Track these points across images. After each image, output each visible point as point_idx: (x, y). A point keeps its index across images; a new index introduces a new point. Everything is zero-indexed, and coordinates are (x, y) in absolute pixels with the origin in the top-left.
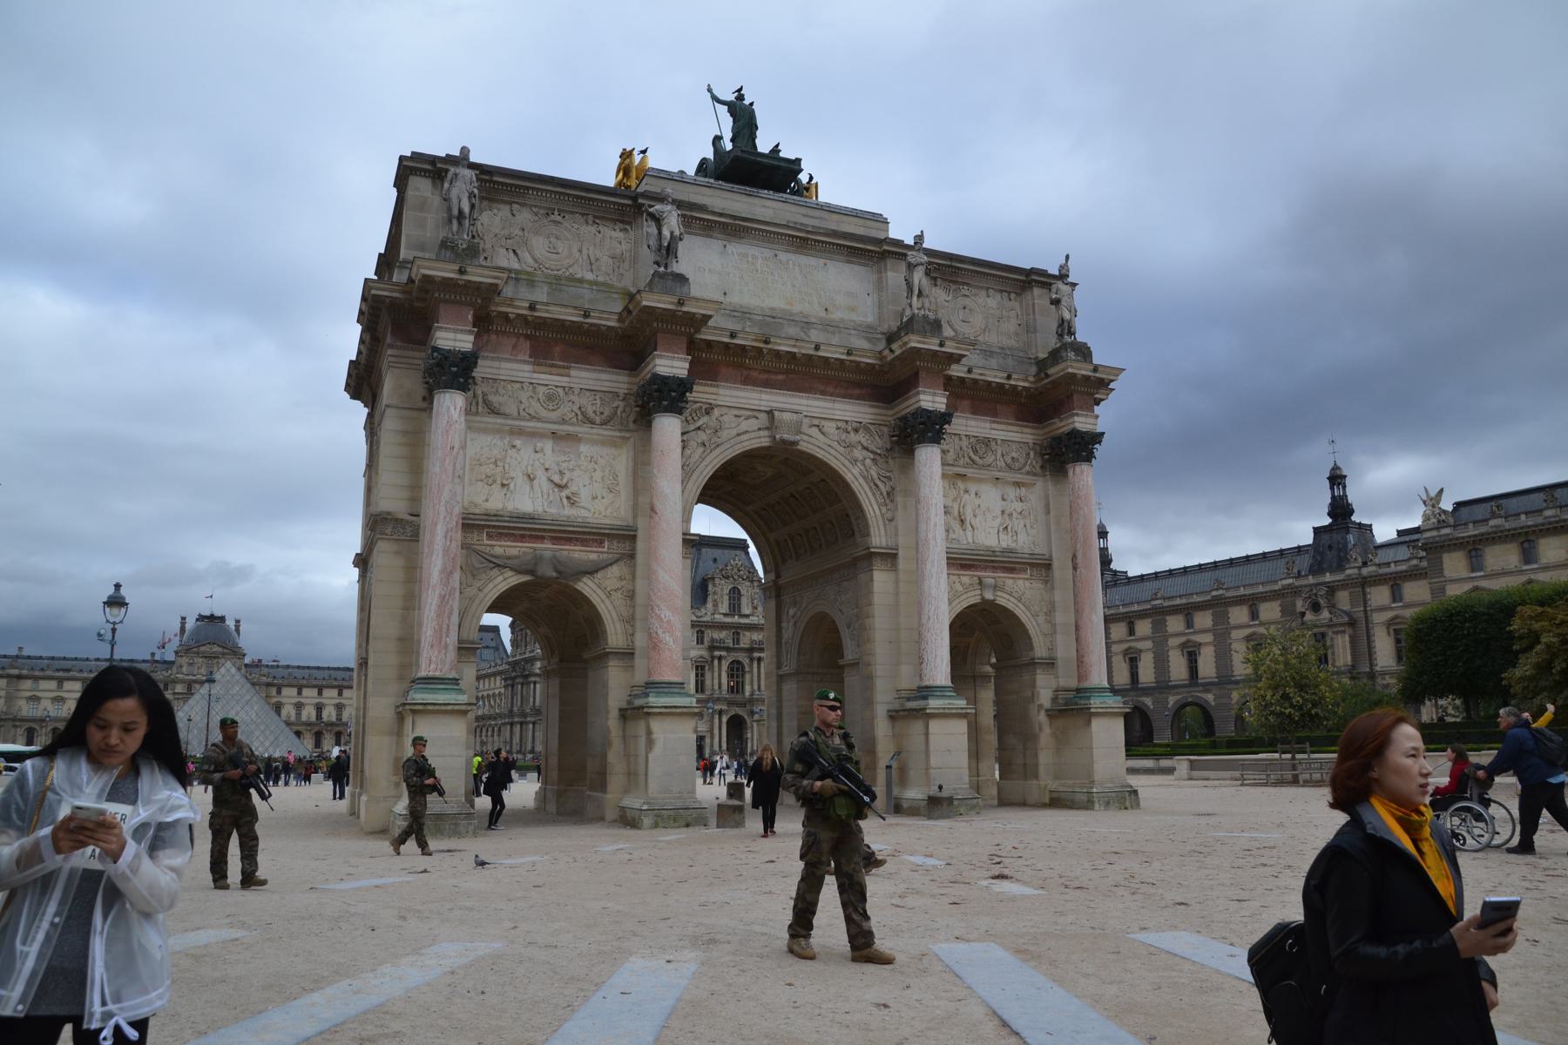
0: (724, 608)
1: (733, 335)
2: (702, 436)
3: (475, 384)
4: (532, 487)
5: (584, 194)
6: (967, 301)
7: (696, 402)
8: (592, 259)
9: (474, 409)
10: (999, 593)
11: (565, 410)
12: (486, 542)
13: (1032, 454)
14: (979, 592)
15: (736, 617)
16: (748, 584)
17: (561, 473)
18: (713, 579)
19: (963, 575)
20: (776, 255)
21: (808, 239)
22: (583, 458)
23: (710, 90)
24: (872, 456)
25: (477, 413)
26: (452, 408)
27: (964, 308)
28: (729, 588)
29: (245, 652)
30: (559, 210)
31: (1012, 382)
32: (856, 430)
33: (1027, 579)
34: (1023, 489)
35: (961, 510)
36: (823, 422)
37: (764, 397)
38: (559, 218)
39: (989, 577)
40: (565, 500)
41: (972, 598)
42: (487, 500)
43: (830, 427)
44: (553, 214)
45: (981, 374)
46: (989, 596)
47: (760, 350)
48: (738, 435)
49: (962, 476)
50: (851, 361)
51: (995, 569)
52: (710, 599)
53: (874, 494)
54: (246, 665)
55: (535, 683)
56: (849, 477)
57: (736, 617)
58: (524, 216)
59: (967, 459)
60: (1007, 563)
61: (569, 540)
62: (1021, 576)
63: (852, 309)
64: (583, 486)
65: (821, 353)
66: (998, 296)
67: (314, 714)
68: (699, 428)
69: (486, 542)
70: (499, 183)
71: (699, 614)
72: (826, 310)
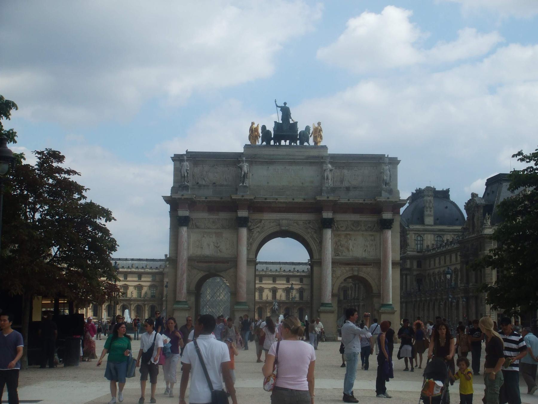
1: (266, 199)
2: (259, 230)
3: (193, 220)
4: (209, 247)
5: (222, 159)
7: (257, 219)
8: (227, 179)
9: (192, 227)
10: (360, 273)
12: (196, 264)
13: (376, 225)
14: (351, 273)
17: (217, 243)
19: (346, 267)
20: (285, 168)
21: (295, 162)
22: (224, 238)
23: (275, 102)
24: (314, 230)
25: (193, 228)
26: (183, 232)
27: (355, 175)
30: (216, 164)
31: (365, 202)
32: (309, 223)
33: (371, 268)
34: (373, 238)
35: (348, 245)
36: (298, 221)
37: (278, 215)
38: (217, 167)
39: (356, 268)
40: (219, 251)
41: (349, 274)
42: (197, 252)
44: (215, 166)
45: (353, 201)
46: (356, 273)
47: (275, 202)
48: (270, 228)
49: (349, 234)
50: (305, 202)
51: (359, 264)
53: (315, 243)
55: (406, 275)
56: (306, 238)
59: (350, 228)
60: (364, 263)
62: (369, 266)
65: (294, 201)
67: (270, 295)
68: (257, 227)
69: (196, 264)
70: (198, 160)
72: (302, 183)
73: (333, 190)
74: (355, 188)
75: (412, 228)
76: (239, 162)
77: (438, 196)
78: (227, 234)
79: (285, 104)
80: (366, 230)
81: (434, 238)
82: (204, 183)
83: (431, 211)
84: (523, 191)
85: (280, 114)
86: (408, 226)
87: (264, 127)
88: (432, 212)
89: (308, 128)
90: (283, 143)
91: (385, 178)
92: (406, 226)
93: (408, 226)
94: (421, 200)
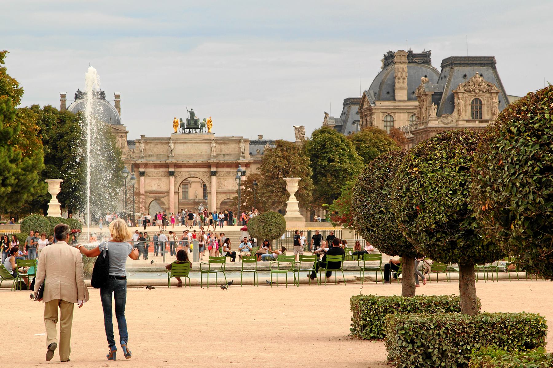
0: (467, 114)
2: (180, 177)
6: (229, 147)
11: (159, 175)
15: (477, 122)
16: (488, 95)
18: (457, 93)
28: (472, 100)
29: (127, 130)
39: (228, 195)
43: (201, 173)
52: (455, 110)
54: (129, 143)
57: (477, 122)
58: (152, 146)
61: (160, 193)
63: (206, 152)
64: (162, 186)
66: (235, 144)
71: (446, 121)
73: (218, 155)
74: (228, 155)
75: (380, 105)
76: (169, 143)
77: (416, 61)
78: (164, 180)
79: (192, 109)
80: (234, 176)
81: (408, 118)
82: (151, 153)
83: (404, 83)
84: (473, 78)
85: (190, 115)
86: (374, 103)
87: (181, 120)
88: (406, 84)
89: (204, 120)
90: (191, 130)
91: (242, 150)
92: (372, 103)
93: (374, 103)
94: (393, 67)
